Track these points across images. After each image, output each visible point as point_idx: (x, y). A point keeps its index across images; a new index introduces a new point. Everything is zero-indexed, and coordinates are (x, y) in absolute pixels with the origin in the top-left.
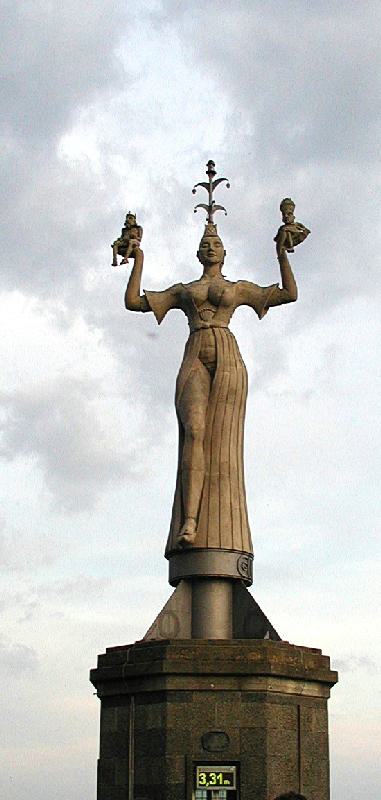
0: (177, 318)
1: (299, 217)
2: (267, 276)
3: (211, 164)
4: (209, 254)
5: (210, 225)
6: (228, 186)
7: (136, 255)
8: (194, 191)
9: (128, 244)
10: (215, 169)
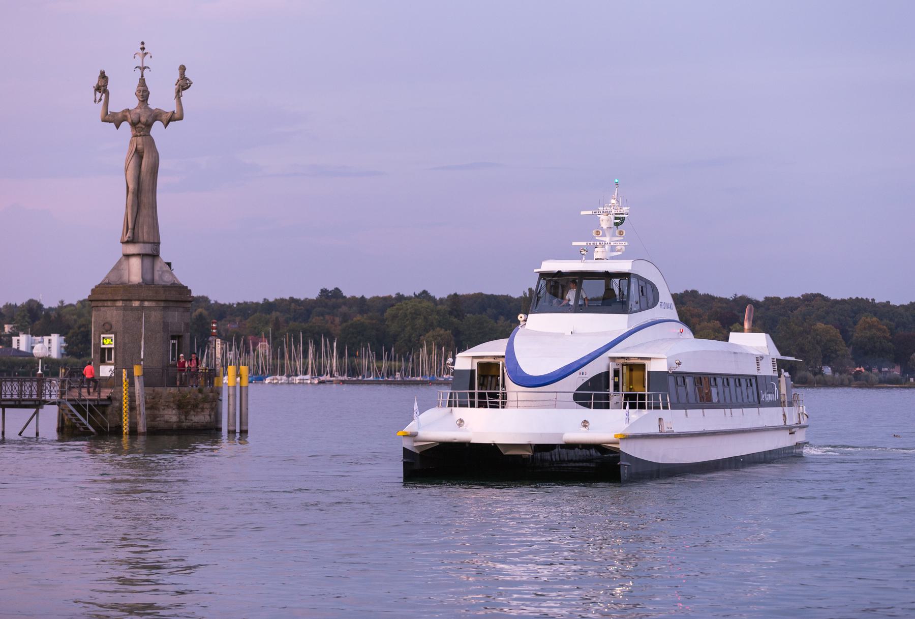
0: (126, 126)
1: (187, 74)
2: (169, 105)
3: (143, 43)
4: (144, 94)
5: (142, 82)
6: (151, 57)
7: (106, 92)
8: (135, 57)
9: (102, 87)
10: (145, 46)
